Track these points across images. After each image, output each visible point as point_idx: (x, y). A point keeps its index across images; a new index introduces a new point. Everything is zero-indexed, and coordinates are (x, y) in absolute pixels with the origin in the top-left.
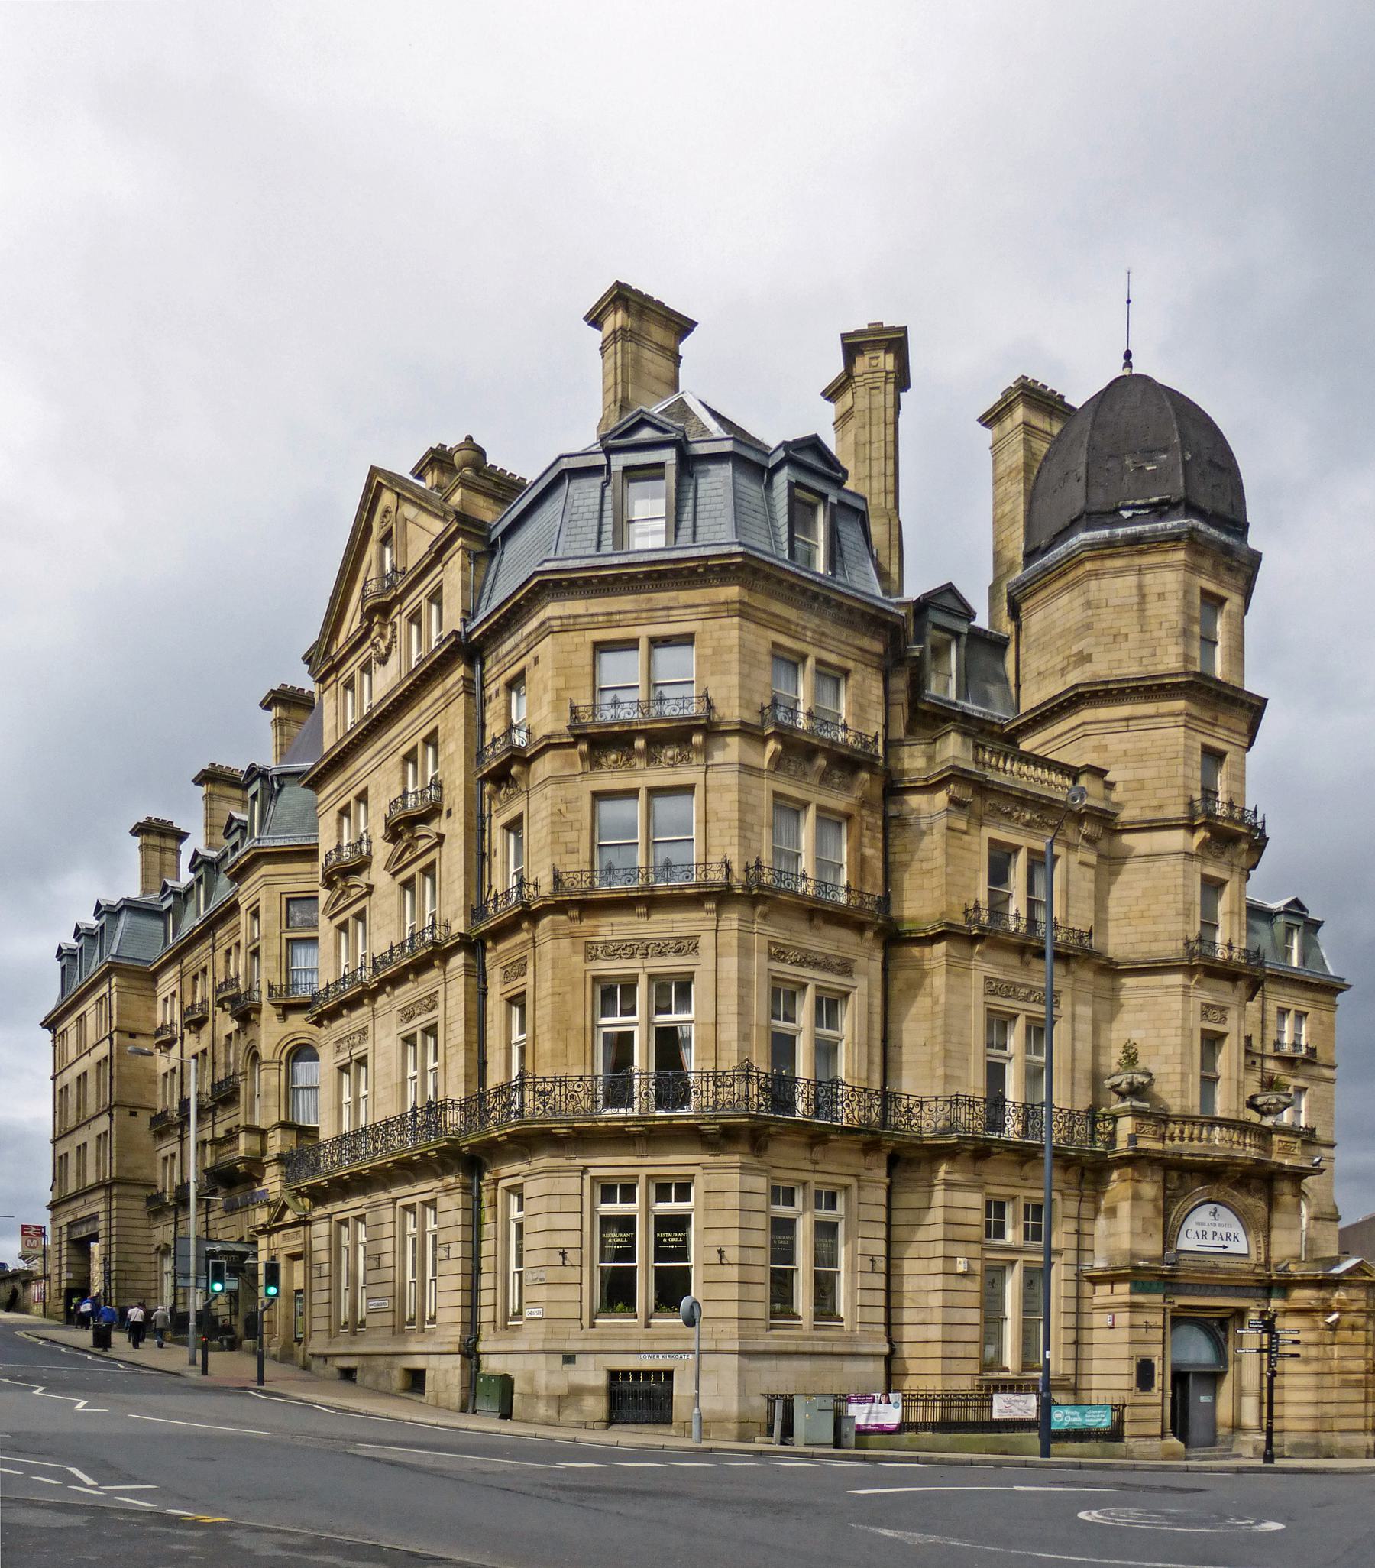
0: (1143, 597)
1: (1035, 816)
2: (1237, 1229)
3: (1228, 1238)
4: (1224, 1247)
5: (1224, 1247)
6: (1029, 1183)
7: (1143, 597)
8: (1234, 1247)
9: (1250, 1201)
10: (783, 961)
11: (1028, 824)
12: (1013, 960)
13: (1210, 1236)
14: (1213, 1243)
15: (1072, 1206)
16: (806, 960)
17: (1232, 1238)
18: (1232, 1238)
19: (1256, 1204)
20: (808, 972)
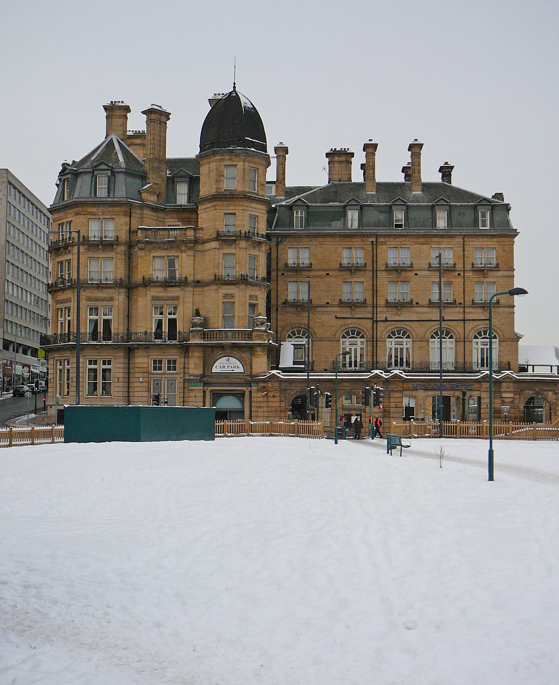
0: (210, 171)
1: (168, 247)
2: (238, 363)
3: (235, 367)
4: (233, 370)
5: (233, 370)
6: (166, 354)
7: (210, 171)
8: (236, 370)
9: (243, 355)
10: (91, 301)
11: (166, 249)
12: (161, 289)
13: (226, 367)
14: (226, 370)
15: (182, 360)
16: (97, 300)
17: (236, 367)
18: (236, 367)
19: (246, 355)
20: (98, 303)
